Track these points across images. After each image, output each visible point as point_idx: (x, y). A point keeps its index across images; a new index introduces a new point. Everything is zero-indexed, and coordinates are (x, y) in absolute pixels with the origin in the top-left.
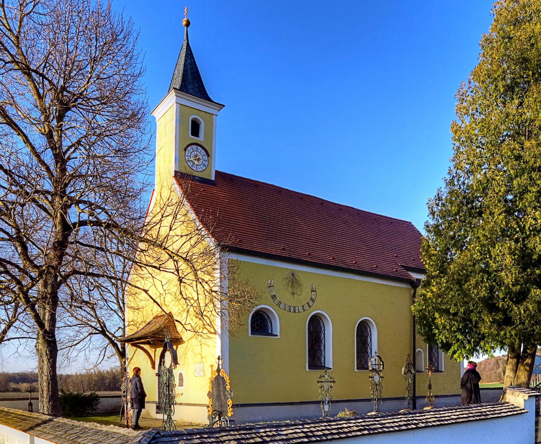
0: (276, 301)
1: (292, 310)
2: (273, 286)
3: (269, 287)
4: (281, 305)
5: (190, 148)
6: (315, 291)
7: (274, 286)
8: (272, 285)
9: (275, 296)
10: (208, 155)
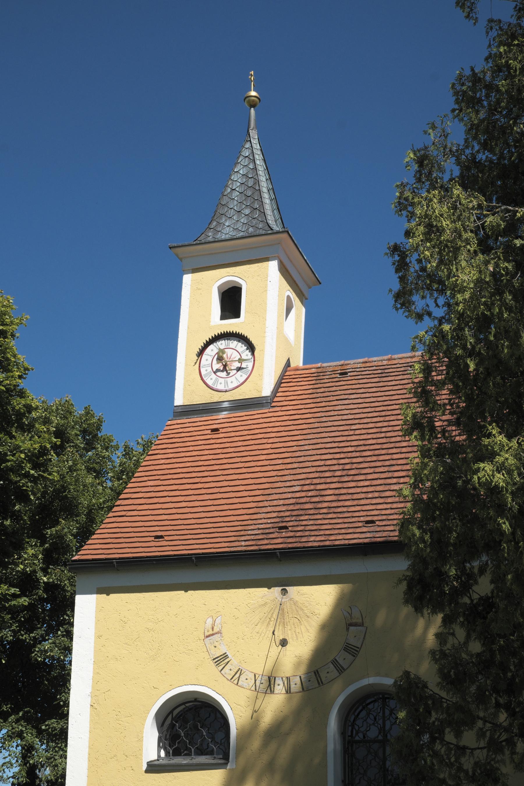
2: (219, 632)
3: (207, 637)
4: (243, 678)
5: (211, 347)
6: (362, 625)
7: (223, 631)
8: (216, 630)
9: (225, 656)
10: (251, 348)
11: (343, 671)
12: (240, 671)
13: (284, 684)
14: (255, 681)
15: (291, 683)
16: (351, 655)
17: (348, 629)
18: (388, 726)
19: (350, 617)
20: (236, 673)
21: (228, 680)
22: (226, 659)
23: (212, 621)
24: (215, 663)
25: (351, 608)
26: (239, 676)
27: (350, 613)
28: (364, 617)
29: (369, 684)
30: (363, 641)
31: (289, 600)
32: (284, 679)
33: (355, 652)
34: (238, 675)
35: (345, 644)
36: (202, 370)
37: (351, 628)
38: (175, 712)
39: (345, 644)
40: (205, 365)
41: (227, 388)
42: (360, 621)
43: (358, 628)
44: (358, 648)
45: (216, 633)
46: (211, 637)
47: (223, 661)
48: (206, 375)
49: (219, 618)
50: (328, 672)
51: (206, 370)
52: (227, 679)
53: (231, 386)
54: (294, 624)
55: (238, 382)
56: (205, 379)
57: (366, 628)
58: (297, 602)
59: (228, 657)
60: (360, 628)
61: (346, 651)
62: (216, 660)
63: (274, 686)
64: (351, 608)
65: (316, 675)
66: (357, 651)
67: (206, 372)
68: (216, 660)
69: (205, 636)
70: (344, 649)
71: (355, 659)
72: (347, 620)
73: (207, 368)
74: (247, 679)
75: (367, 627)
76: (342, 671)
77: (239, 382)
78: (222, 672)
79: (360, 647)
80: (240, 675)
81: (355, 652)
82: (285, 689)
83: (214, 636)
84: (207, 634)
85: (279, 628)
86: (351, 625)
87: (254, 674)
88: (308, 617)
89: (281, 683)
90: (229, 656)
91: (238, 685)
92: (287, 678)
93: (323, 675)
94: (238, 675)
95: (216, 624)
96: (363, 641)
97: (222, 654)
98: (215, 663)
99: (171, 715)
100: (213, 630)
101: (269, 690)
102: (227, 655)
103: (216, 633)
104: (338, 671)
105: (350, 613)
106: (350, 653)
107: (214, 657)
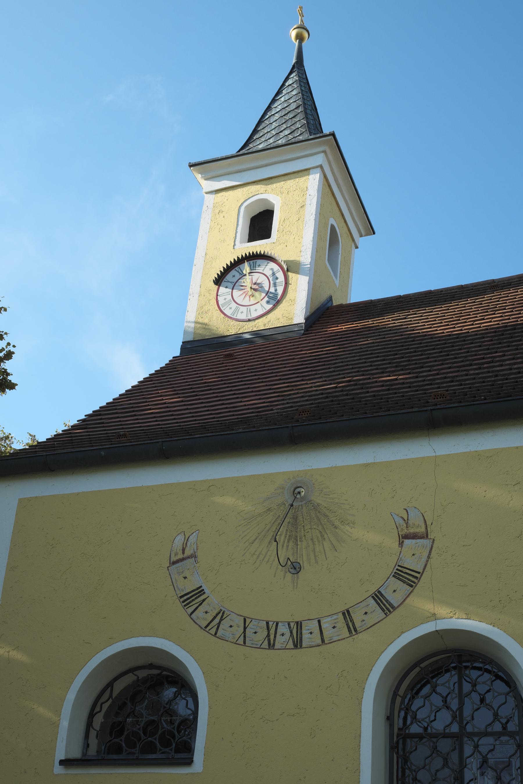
0: (200, 612)
1: (280, 641)
2: (194, 556)
3: (174, 563)
4: (225, 624)
6: (425, 536)
7: (199, 554)
8: (188, 552)
9: (199, 591)
11: (392, 610)
12: (221, 615)
13: (291, 632)
14: (245, 628)
15: (304, 632)
16: (405, 585)
17: (401, 544)
18: (467, 711)
19: (405, 525)
20: (215, 618)
21: (201, 628)
22: (201, 595)
23: (183, 539)
24: (183, 602)
25: (407, 511)
26: (220, 622)
27: (406, 519)
28: (429, 523)
29: (437, 631)
30: (427, 561)
31: (306, 503)
32: (292, 625)
33: (413, 579)
34: (217, 620)
35: (397, 567)
36: (219, 298)
37: (407, 542)
38: (119, 686)
39: (397, 567)
40: (224, 293)
41: (249, 317)
42: (423, 530)
43: (418, 541)
44: (419, 573)
45: (188, 557)
46: (180, 564)
47: (196, 598)
48: (223, 305)
49: (194, 534)
50: (366, 613)
51: (225, 299)
52: (200, 626)
53: (254, 315)
54: (312, 540)
55: (264, 309)
56: (222, 309)
57: (432, 541)
58: (319, 505)
59: (204, 593)
60: (422, 540)
61: (398, 579)
62: (185, 598)
63: (275, 637)
64: (407, 511)
65: (345, 618)
66: (416, 578)
67: (224, 301)
68: (185, 598)
69: (172, 561)
70: (394, 576)
71: (412, 592)
72: (399, 530)
73: (226, 297)
74: (231, 626)
75: (434, 540)
76: (390, 611)
77: (266, 309)
78: (193, 616)
79: (421, 571)
80: (221, 620)
81: (413, 579)
82: (294, 642)
83: (185, 562)
84: (174, 559)
85: (288, 546)
86: (407, 537)
87: (243, 618)
88: (336, 527)
89: (287, 632)
90: (205, 591)
91: (217, 635)
92: (297, 623)
93: (357, 617)
94: (217, 620)
95: (188, 544)
96: (427, 561)
97: (195, 588)
98: (183, 602)
99: (108, 691)
100: (183, 553)
101: (266, 642)
102: (203, 590)
103: (188, 557)
104: (383, 610)
105: (406, 519)
106: (404, 582)
107: (183, 594)
